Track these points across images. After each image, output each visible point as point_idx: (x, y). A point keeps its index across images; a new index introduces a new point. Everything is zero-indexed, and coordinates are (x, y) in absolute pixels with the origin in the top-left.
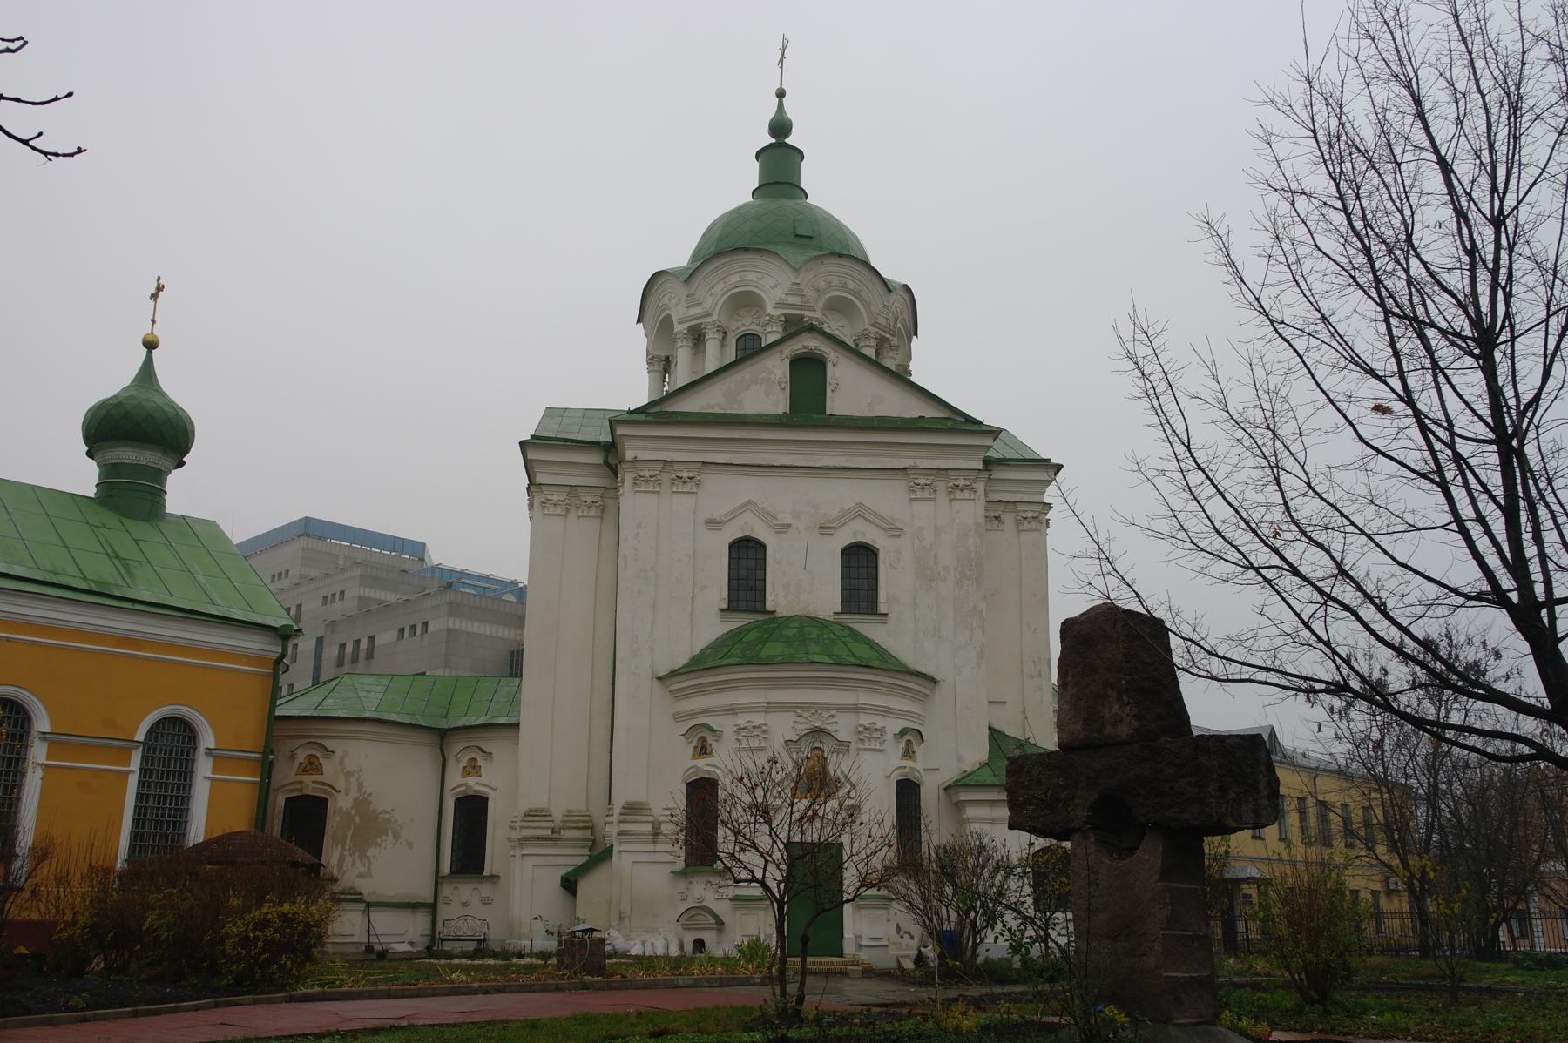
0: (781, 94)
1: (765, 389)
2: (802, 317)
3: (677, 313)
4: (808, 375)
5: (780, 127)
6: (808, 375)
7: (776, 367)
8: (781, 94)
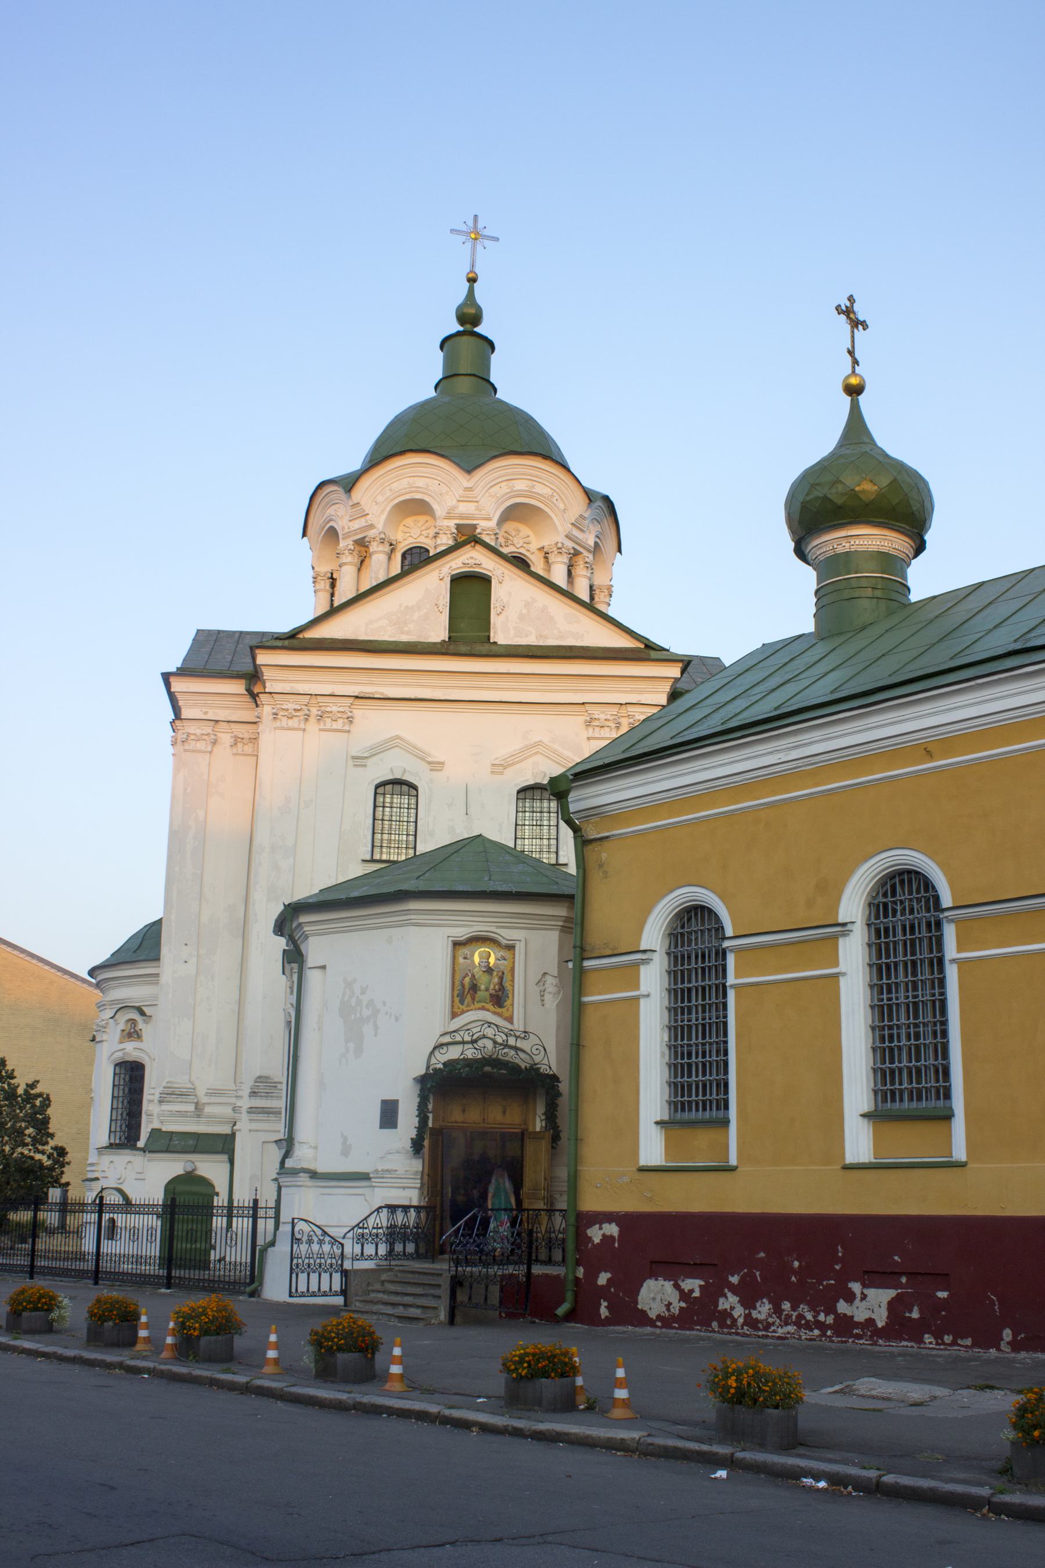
0: (472, 280)
1: (421, 607)
2: (475, 527)
3: (343, 525)
4: (470, 592)
5: (469, 316)
6: (470, 592)
7: (431, 588)
8: (472, 280)
